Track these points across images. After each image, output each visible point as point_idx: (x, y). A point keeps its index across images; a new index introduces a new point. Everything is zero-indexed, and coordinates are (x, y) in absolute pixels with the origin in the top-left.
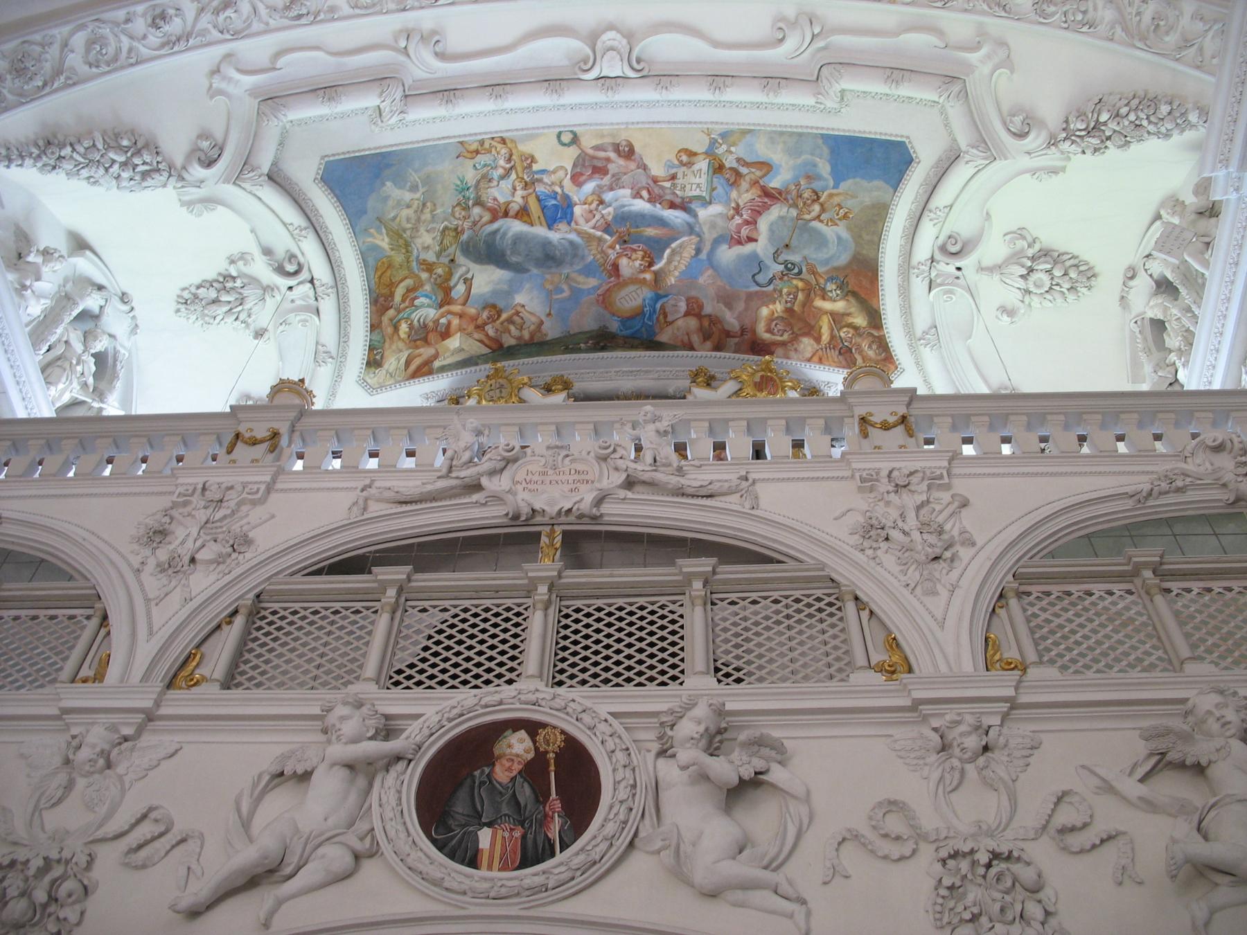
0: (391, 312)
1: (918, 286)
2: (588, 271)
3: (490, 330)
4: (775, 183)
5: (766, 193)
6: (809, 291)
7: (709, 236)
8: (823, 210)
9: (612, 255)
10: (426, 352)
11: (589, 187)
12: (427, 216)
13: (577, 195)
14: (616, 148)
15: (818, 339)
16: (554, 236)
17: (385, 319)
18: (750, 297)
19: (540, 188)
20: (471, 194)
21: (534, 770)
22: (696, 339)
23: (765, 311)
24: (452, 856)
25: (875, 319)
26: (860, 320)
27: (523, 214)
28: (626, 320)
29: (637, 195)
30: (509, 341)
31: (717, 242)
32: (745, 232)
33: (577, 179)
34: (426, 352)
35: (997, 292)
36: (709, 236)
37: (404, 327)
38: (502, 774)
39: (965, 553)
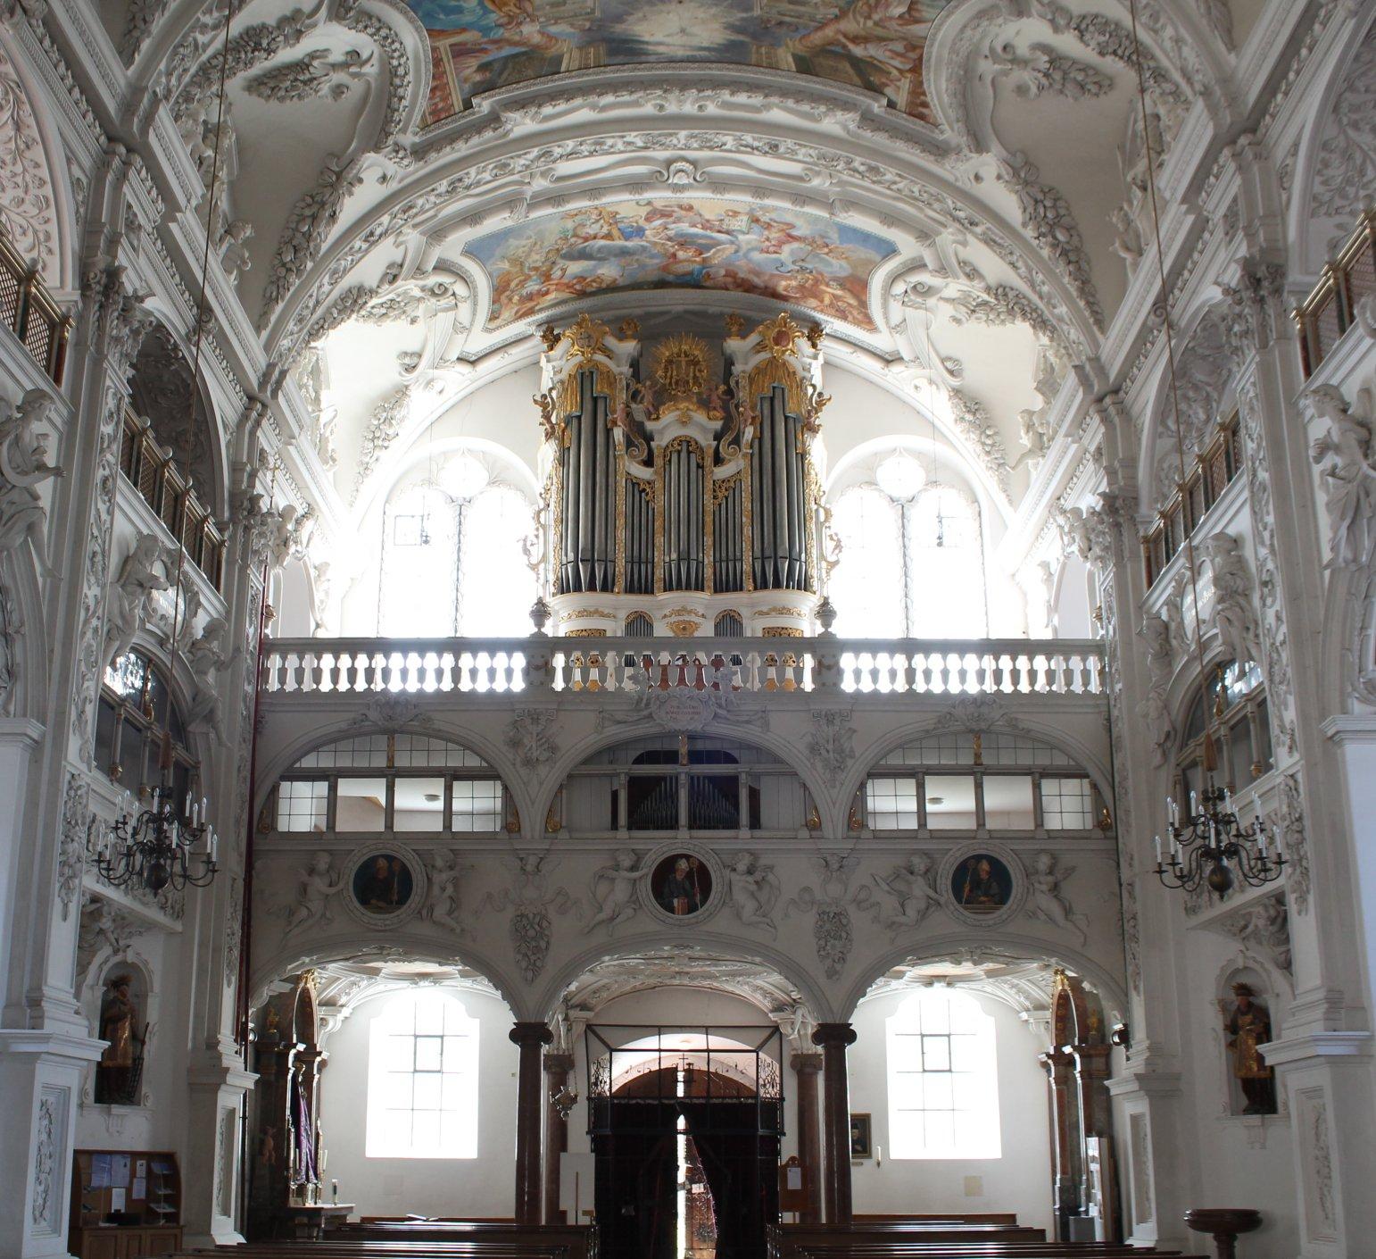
0: (507, 293)
1: (895, 306)
2: (653, 257)
3: (578, 287)
4: (795, 233)
5: (789, 236)
6: (816, 282)
7: (744, 248)
8: (831, 251)
9: (672, 250)
10: (530, 305)
11: (658, 223)
12: (538, 247)
13: (646, 226)
14: (680, 207)
15: (822, 301)
16: (629, 244)
17: (503, 298)
18: (773, 275)
19: (620, 225)
20: (570, 233)
21: (689, 875)
22: (731, 287)
23: (784, 283)
24: (666, 909)
25: (863, 304)
26: (853, 302)
27: (608, 236)
28: (678, 276)
29: (694, 226)
30: (589, 290)
31: (749, 250)
32: (771, 249)
33: (648, 219)
34: (530, 305)
35: (948, 310)
36: (744, 248)
37: (516, 298)
38: (679, 877)
39: (850, 762)
